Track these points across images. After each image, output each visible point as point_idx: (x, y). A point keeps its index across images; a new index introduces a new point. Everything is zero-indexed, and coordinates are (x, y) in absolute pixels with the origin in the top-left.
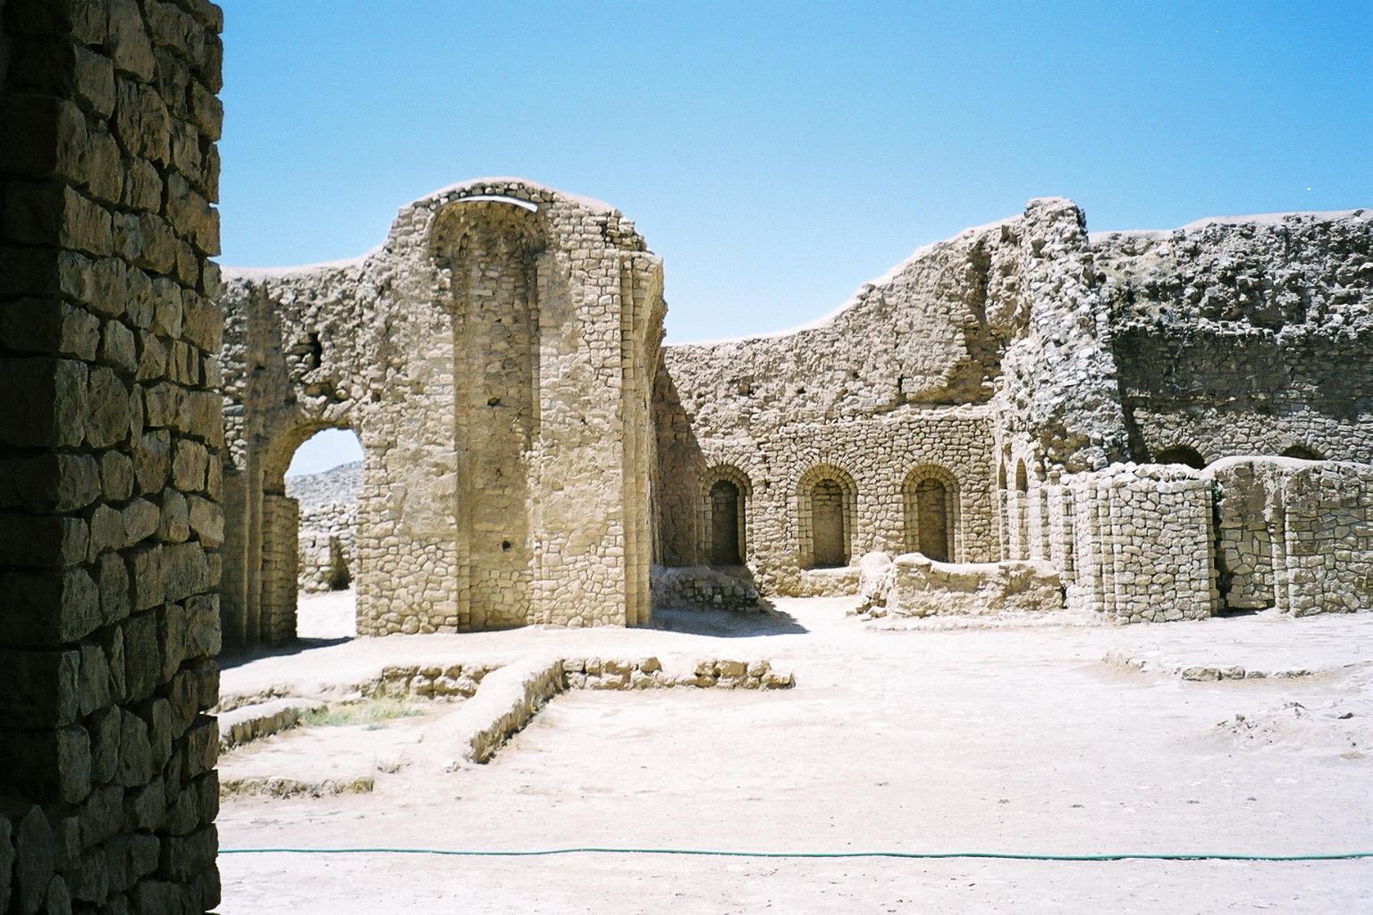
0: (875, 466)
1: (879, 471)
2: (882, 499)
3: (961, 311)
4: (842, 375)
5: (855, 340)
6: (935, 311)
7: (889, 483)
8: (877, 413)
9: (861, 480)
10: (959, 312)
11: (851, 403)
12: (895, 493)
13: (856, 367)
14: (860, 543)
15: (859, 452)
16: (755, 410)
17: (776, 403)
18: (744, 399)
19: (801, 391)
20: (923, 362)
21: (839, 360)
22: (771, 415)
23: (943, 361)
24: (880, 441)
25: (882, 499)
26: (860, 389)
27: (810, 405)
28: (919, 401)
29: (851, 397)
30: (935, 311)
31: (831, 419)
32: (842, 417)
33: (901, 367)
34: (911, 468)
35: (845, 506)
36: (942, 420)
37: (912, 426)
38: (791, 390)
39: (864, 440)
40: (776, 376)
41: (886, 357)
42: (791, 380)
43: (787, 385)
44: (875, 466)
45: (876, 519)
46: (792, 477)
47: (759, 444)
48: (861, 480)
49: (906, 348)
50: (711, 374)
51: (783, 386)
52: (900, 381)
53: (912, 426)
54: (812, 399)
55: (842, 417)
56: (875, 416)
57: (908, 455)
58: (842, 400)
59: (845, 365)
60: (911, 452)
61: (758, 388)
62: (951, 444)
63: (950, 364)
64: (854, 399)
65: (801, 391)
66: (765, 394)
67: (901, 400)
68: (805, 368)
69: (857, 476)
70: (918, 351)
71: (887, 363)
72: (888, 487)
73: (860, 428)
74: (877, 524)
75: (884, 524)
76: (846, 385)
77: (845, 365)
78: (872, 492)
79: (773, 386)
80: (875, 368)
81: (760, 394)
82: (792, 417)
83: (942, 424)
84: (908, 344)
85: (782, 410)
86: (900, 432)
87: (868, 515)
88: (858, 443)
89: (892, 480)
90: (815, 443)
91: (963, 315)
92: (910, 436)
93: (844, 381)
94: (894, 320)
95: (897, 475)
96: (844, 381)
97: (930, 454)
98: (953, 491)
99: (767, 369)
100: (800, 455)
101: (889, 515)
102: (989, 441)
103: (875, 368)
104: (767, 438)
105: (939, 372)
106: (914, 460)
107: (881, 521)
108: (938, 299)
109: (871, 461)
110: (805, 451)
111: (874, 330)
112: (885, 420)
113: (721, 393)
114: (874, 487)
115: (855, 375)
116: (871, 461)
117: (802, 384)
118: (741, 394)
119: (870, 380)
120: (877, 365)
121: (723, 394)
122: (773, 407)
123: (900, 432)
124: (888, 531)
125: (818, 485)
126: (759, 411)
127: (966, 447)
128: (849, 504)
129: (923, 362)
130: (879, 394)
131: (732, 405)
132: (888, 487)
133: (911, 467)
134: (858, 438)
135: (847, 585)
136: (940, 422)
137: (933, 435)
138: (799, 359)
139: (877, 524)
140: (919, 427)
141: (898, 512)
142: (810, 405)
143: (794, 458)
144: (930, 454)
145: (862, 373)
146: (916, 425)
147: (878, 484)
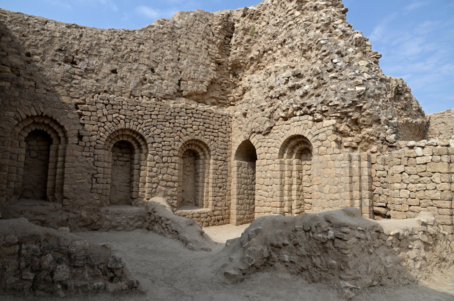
0: (162, 135)
1: (165, 139)
2: (164, 159)
3: (214, 50)
4: (144, 68)
5: (154, 48)
6: (201, 46)
7: (170, 148)
8: (165, 99)
9: (152, 143)
10: (213, 51)
11: (148, 88)
12: (174, 155)
13: (154, 65)
14: (147, 190)
15: (153, 123)
16: (76, 77)
17: (94, 75)
18: (68, 66)
19: (114, 71)
20: (194, 73)
21: (143, 57)
22: (89, 83)
23: (204, 76)
24: (167, 118)
25: (164, 159)
26: (155, 80)
27: (120, 83)
28: (188, 96)
29: (149, 84)
30: (201, 46)
31: (134, 97)
32: (142, 97)
33: (181, 72)
34: (186, 140)
35: (136, 161)
36: (205, 111)
37: (188, 111)
38: (107, 69)
39: (157, 115)
40: (96, 55)
41: (172, 64)
42: (108, 61)
43: (104, 64)
44: (162, 135)
45: (160, 173)
46: (102, 134)
47: (77, 104)
48: (152, 143)
49: (185, 62)
50: (41, 40)
51: (102, 64)
52: (180, 81)
53: (188, 111)
54: (122, 79)
55: (142, 97)
56: (163, 101)
57: (183, 130)
58: (143, 84)
59: (147, 62)
60: (186, 128)
61: (80, 60)
62: (209, 128)
63: (208, 79)
64: (151, 86)
65: (114, 71)
66: (85, 67)
67: (179, 94)
68: (119, 56)
69: (149, 140)
70: (191, 66)
71: (173, 68)
72: (169, 151)
73: (155, 106)
74: (160, 177)
75: (165, 177)
76: (146, 75)
77: (147, 62)
78: (160, 153)
79: (94, 61)
80: (166, 69)
81: (82, 65)
82: (106, 88)
83: (205, 114)
84: (187, 60)
85: (97, 80)
86: (180, 114)
87: (155, 169)
88: (153, 117)
89: (173, 146)
90: (122, 111)
91: (215, 53)
92: (186, 118)
93: (145, 72)
94: (178, 43)
95: (176, 143)
96: (145, 72)
97: (197, 132)
98: (206, 158)
99: (90, 49)
100: (110, 117)
101: (169, 171)
102: (229, 130)
103: (166, 69)
104: (84, 100)
105: (202, 82)
106: (187, 135)
107: (163, 174)
108: (203, 39)
109: (160, 131)
110: (114, 115)
111: (166, 45)
112: (171, 104)
113: (49, 57)
114: (161, 150)
115: (153, 70)
116: (160, 131)
117: (116, 67)
118: (66, 61)
119: (163, 76)
120: (167, 68)
121: (49, 58)
122: (91, 78)
123: (180, 114)
124: (167, 182)
125: (115, 146)
126: (80, 78)
127: (217, 131)
128: (140, 160)
129: (194, 73)
130: (167, 86)
131: (57, 69)
132: (169, 151)
133: (186, 138)
134: (153, 113)
135: (137, 221)
136: (205, 111)
137: (199, 120)
138: (115, 48)
139: (160, 177)
140: (192, 113)
141: (175, 169)
142: (120, 83)
143: (104, 119)
144: (197, 132)
145: (157, 70)
146: (190, 111)
147: (164, 148)
